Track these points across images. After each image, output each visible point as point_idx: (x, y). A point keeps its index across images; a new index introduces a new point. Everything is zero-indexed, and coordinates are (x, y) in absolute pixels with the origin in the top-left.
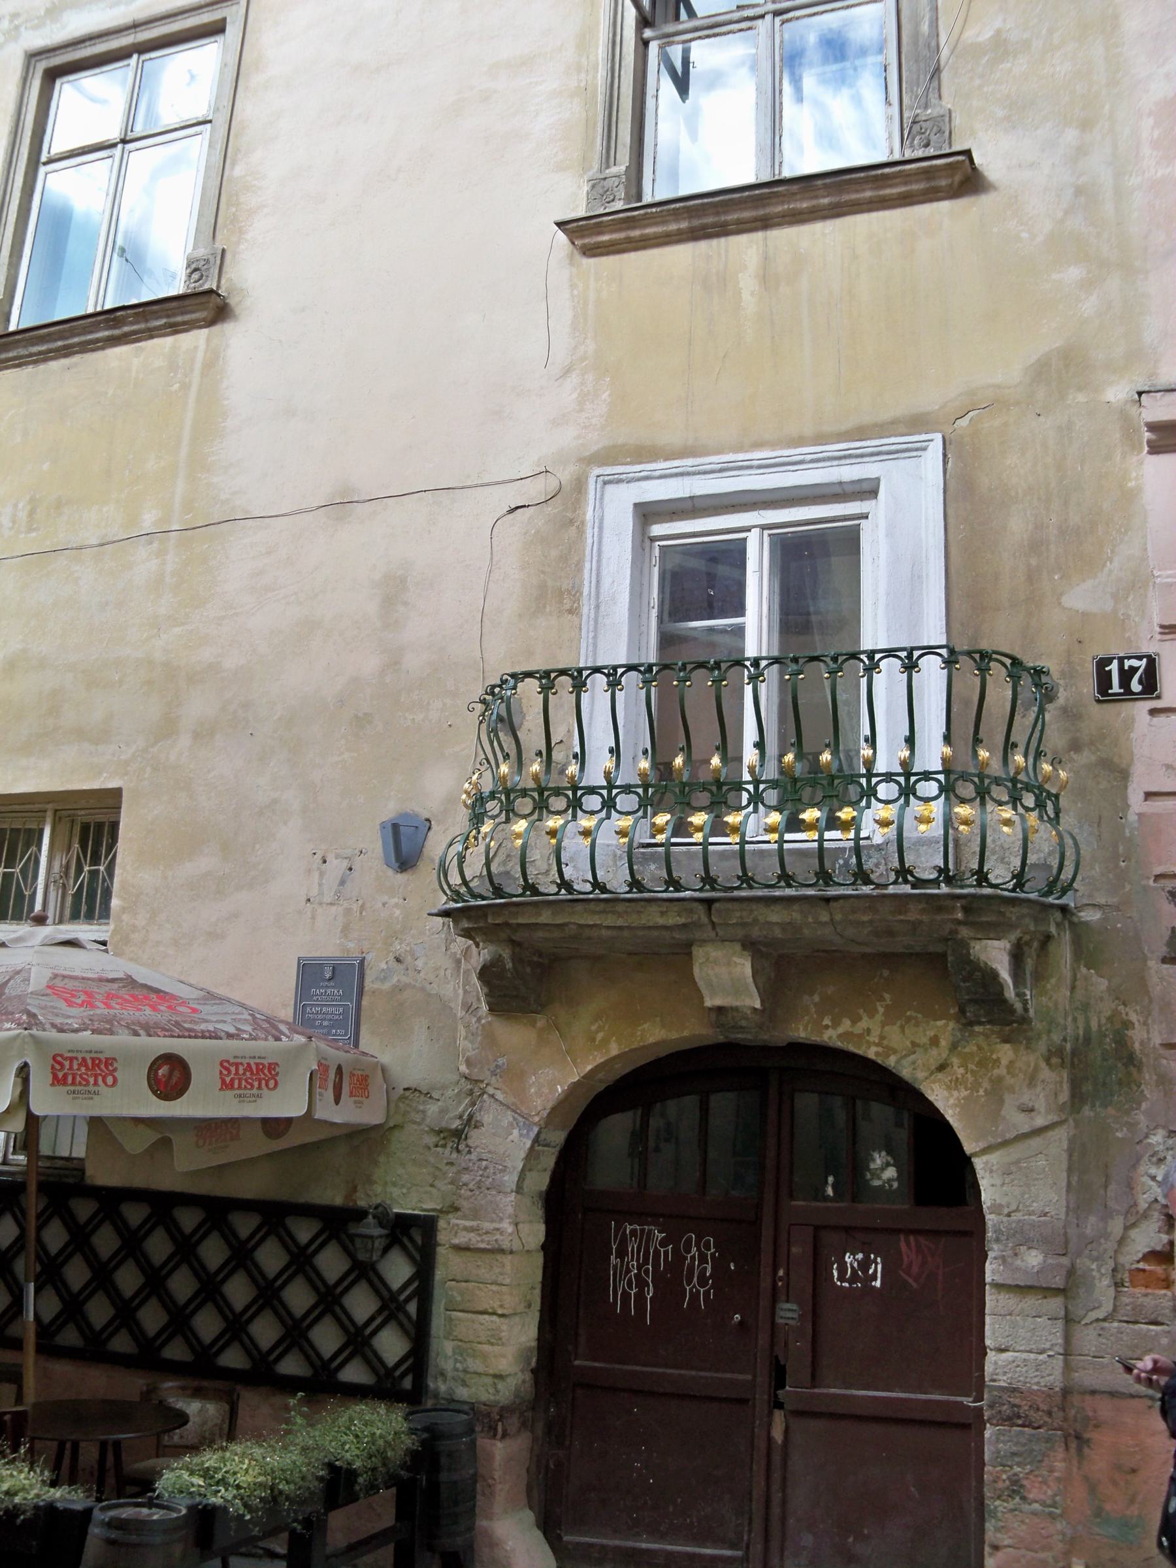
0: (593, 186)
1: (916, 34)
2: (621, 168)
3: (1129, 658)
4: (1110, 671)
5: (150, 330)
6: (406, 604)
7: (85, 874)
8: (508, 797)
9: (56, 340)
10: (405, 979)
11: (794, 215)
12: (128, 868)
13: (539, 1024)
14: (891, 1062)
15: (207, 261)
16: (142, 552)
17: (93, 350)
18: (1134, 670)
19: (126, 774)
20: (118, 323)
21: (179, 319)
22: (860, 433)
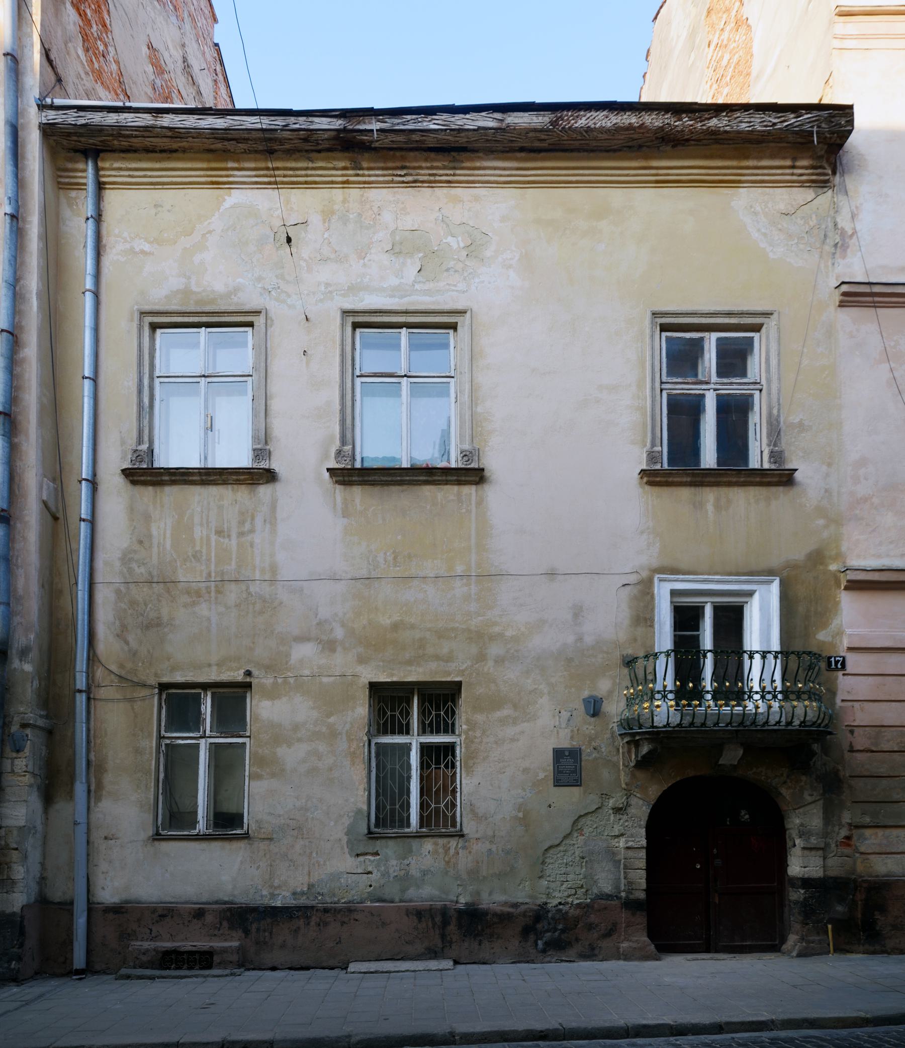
0: (648, 454)
5: (447, 481)
6: (583, 617)
9: (396, 476)
10: (598, 755)
12: (469, 713)
15: (471, 453)
16: (458, 583)
17: (414, 485)
19: (464, 675)
21: (463, 478)
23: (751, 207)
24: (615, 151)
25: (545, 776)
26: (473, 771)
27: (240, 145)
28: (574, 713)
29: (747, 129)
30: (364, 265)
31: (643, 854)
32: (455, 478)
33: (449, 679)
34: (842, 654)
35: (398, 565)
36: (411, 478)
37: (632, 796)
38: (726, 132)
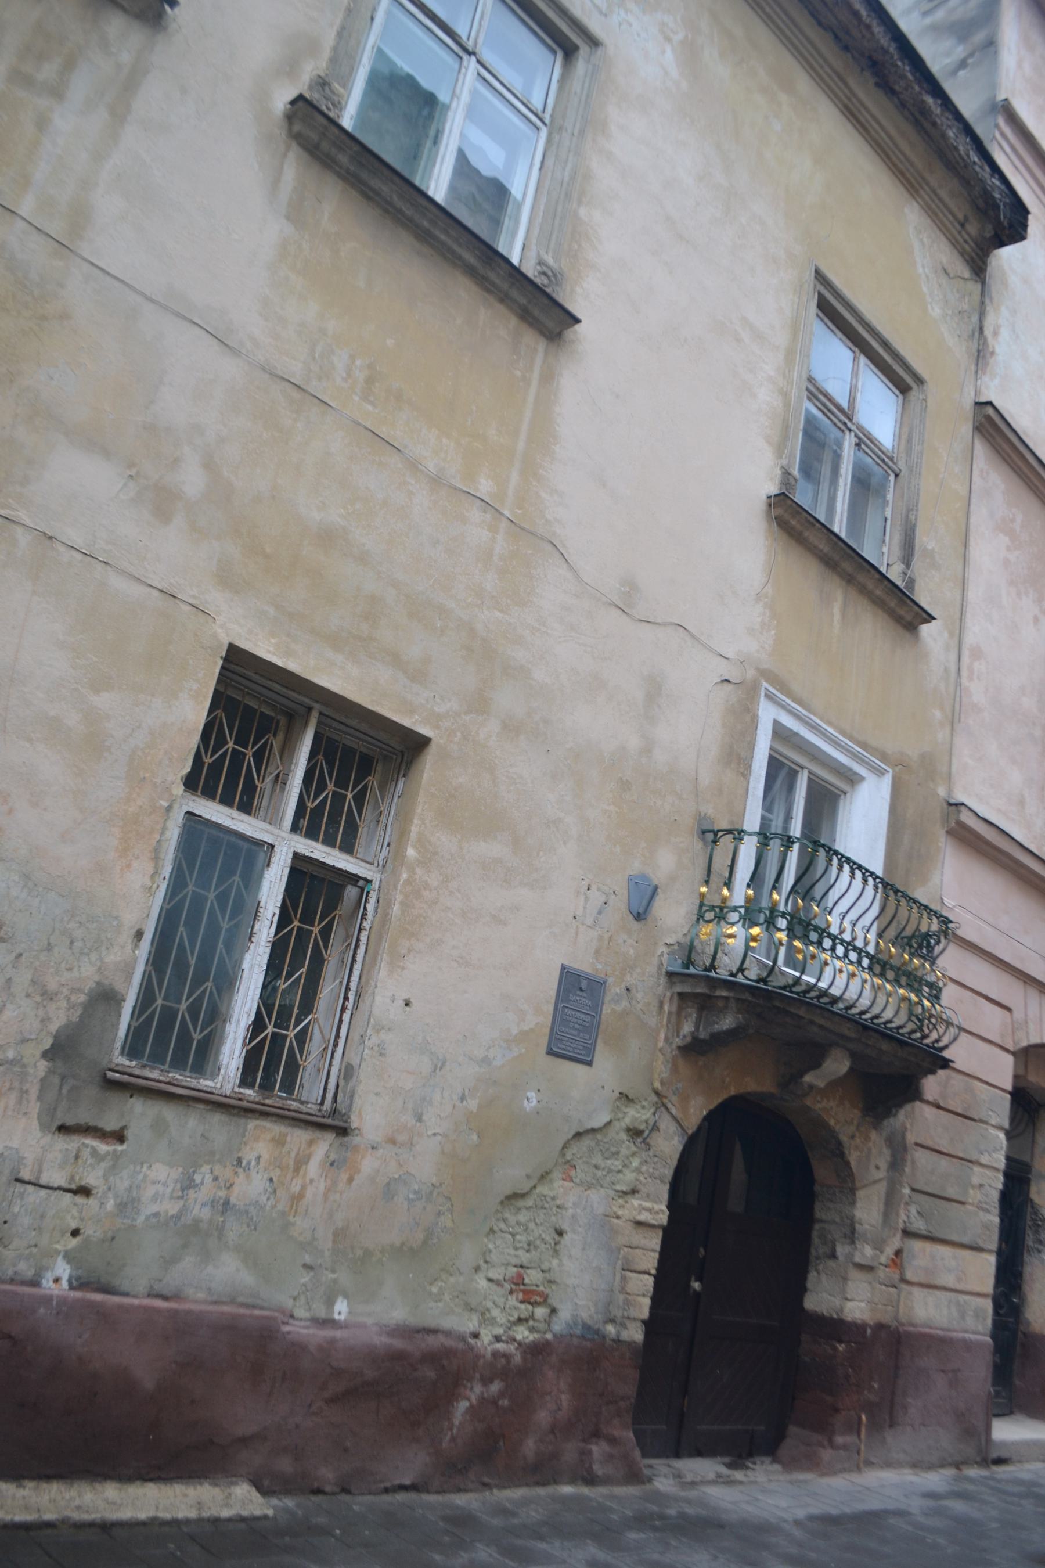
5: (506, 295)
6: (659, 707)
13: (701, 1063)
14: (837, 1128)
16: (475, 514)
19: (438, 727)
24: (820, 24)
25: (537, 1024)
26: (403, 968)
32: (523, 301)
33: (407, 722)
35: (372, 399)
36: (450, 242)
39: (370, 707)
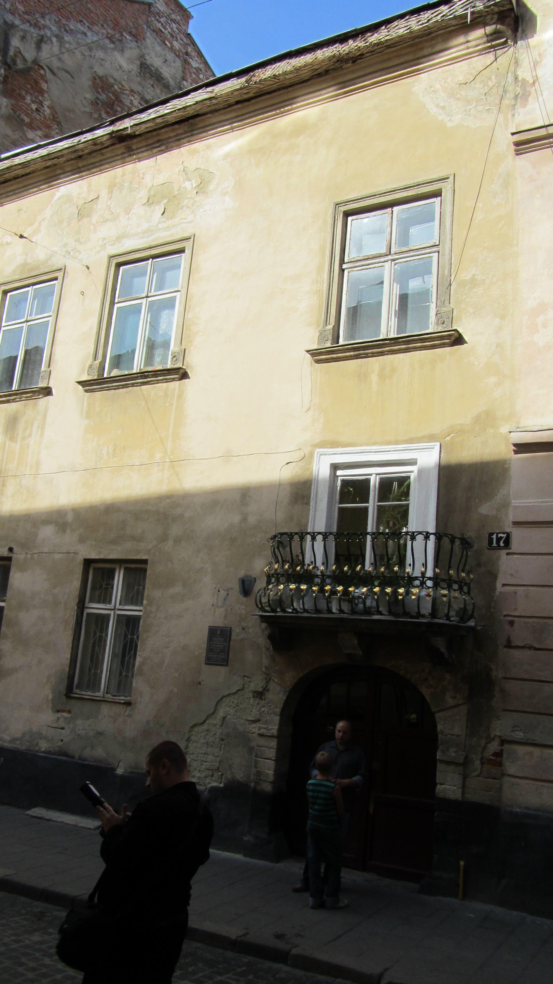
0: (321, 334)
1: (443, 274)
2: (330, 327)
3: (500, 533)
4: (493, 538)
6: (250, 497)
7: (135, 589)
8: (277, 576)
11: (392, 351)
15: (179, 353)
18: (501, 538)
20: (146, 377)
22: (411, 441)
23: (431, 87)
27: (60, 159)
28: (230, 593)
29: (406, 32)
30: (129, 218)
31: (274, 743)
34: (508, 530)
37: (271, 680)
38: (389, 40)
39: (126, 558)
